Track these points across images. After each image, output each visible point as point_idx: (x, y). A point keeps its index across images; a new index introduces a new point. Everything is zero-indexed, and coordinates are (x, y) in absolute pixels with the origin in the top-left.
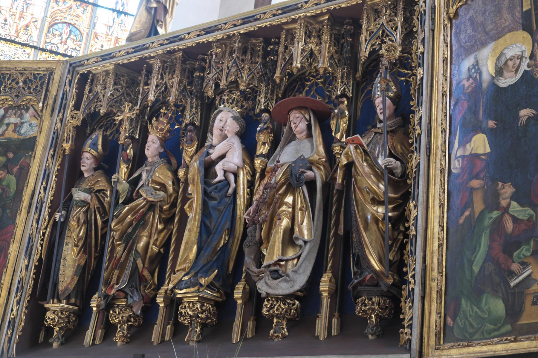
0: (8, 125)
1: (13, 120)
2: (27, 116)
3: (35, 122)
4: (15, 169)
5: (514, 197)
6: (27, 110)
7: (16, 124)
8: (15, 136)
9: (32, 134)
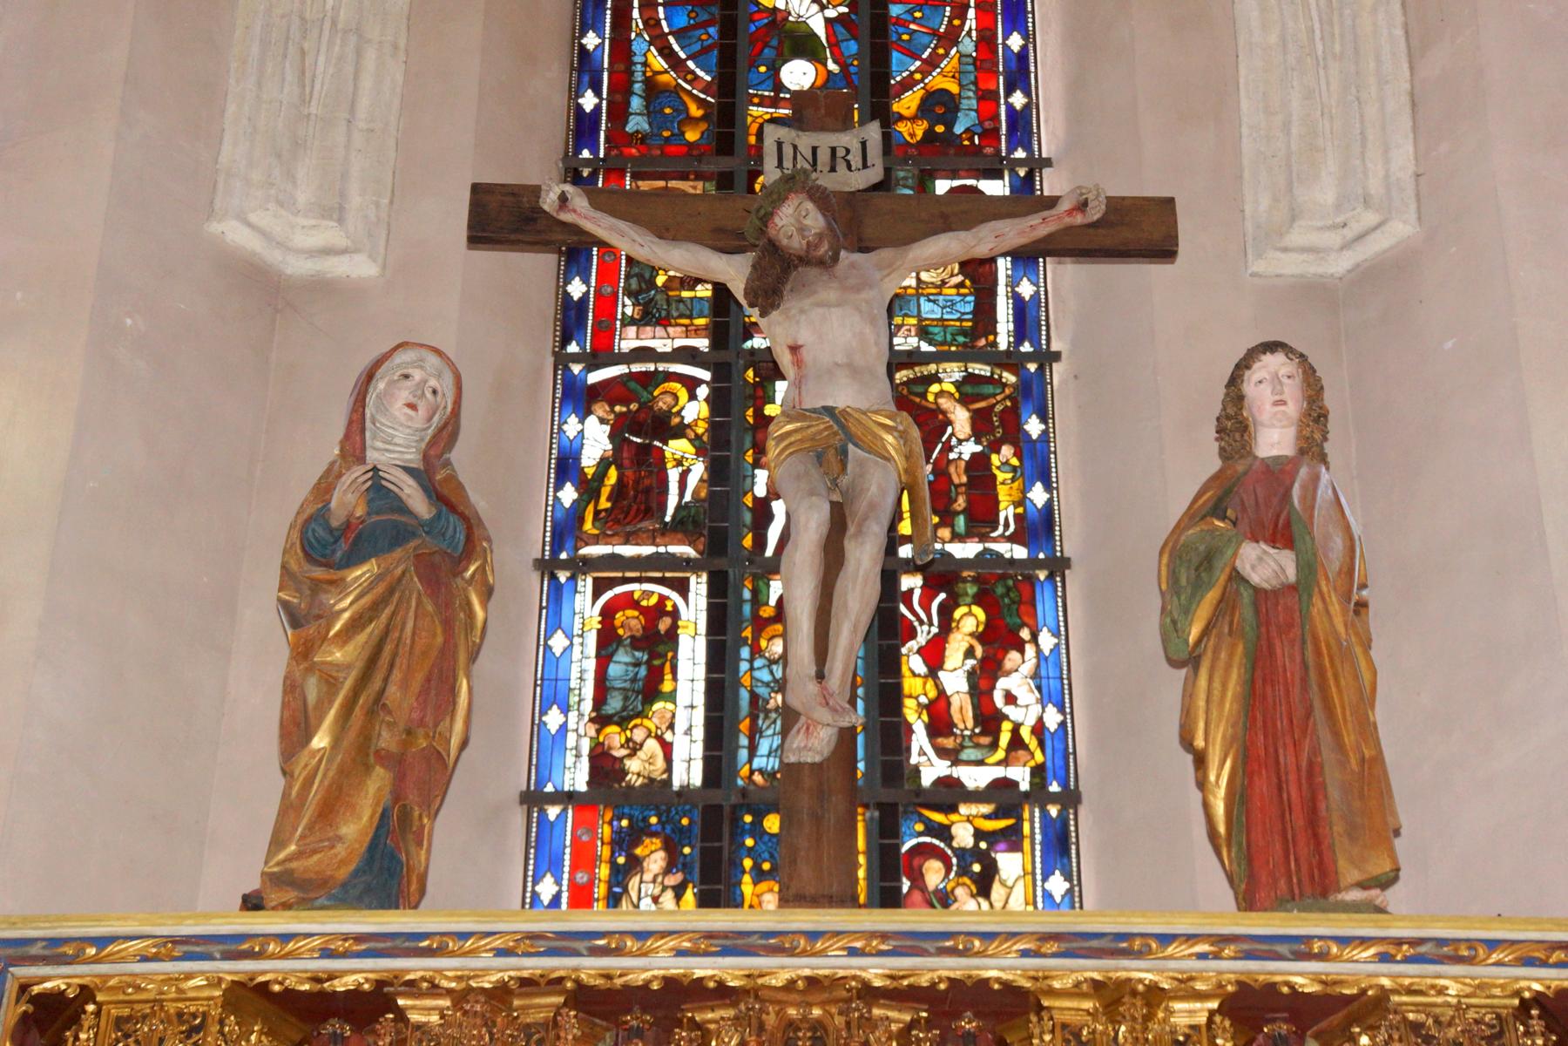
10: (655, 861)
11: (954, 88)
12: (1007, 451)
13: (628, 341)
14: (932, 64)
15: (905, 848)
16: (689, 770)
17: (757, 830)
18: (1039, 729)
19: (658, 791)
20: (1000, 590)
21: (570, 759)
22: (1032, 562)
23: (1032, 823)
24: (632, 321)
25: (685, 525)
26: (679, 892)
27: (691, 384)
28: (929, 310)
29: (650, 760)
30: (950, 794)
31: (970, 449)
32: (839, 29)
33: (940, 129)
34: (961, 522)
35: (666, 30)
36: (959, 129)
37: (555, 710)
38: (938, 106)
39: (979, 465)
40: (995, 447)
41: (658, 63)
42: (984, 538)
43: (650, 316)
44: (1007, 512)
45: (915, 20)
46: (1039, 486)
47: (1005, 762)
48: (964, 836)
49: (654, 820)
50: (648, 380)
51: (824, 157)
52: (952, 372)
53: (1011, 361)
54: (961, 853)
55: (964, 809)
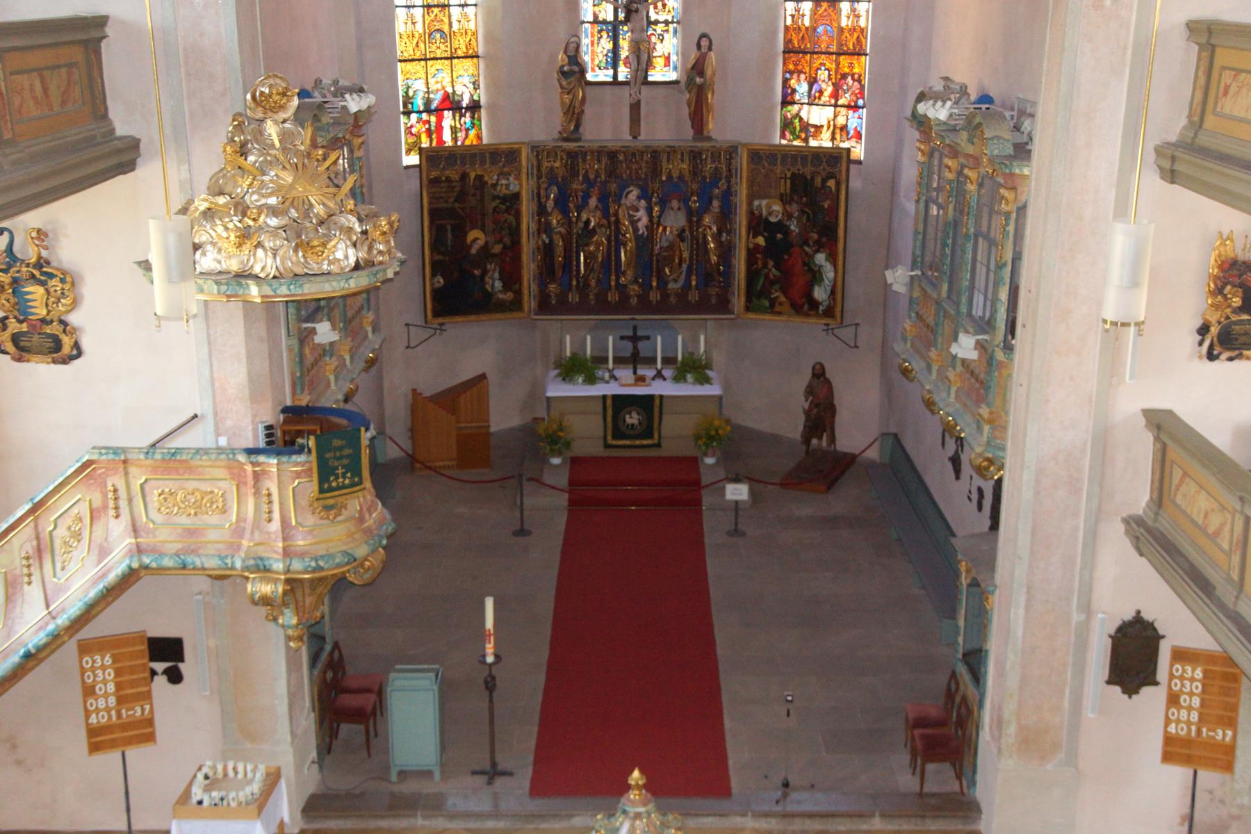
0: (502, 185)
1: (504, 182)
2: (511, 179)
3: (516, 182)
4: (513, 212)
5: (774, 266)
6: (510, 175)
7: (506, 185)
8: (507, 192)
9: (517, 189)
10: (604, 34)
15: (649, 33)
16: (610, 18)
17: (623, 30)
18: (673, 8)
19: (605, 22)
30: (656, 22)
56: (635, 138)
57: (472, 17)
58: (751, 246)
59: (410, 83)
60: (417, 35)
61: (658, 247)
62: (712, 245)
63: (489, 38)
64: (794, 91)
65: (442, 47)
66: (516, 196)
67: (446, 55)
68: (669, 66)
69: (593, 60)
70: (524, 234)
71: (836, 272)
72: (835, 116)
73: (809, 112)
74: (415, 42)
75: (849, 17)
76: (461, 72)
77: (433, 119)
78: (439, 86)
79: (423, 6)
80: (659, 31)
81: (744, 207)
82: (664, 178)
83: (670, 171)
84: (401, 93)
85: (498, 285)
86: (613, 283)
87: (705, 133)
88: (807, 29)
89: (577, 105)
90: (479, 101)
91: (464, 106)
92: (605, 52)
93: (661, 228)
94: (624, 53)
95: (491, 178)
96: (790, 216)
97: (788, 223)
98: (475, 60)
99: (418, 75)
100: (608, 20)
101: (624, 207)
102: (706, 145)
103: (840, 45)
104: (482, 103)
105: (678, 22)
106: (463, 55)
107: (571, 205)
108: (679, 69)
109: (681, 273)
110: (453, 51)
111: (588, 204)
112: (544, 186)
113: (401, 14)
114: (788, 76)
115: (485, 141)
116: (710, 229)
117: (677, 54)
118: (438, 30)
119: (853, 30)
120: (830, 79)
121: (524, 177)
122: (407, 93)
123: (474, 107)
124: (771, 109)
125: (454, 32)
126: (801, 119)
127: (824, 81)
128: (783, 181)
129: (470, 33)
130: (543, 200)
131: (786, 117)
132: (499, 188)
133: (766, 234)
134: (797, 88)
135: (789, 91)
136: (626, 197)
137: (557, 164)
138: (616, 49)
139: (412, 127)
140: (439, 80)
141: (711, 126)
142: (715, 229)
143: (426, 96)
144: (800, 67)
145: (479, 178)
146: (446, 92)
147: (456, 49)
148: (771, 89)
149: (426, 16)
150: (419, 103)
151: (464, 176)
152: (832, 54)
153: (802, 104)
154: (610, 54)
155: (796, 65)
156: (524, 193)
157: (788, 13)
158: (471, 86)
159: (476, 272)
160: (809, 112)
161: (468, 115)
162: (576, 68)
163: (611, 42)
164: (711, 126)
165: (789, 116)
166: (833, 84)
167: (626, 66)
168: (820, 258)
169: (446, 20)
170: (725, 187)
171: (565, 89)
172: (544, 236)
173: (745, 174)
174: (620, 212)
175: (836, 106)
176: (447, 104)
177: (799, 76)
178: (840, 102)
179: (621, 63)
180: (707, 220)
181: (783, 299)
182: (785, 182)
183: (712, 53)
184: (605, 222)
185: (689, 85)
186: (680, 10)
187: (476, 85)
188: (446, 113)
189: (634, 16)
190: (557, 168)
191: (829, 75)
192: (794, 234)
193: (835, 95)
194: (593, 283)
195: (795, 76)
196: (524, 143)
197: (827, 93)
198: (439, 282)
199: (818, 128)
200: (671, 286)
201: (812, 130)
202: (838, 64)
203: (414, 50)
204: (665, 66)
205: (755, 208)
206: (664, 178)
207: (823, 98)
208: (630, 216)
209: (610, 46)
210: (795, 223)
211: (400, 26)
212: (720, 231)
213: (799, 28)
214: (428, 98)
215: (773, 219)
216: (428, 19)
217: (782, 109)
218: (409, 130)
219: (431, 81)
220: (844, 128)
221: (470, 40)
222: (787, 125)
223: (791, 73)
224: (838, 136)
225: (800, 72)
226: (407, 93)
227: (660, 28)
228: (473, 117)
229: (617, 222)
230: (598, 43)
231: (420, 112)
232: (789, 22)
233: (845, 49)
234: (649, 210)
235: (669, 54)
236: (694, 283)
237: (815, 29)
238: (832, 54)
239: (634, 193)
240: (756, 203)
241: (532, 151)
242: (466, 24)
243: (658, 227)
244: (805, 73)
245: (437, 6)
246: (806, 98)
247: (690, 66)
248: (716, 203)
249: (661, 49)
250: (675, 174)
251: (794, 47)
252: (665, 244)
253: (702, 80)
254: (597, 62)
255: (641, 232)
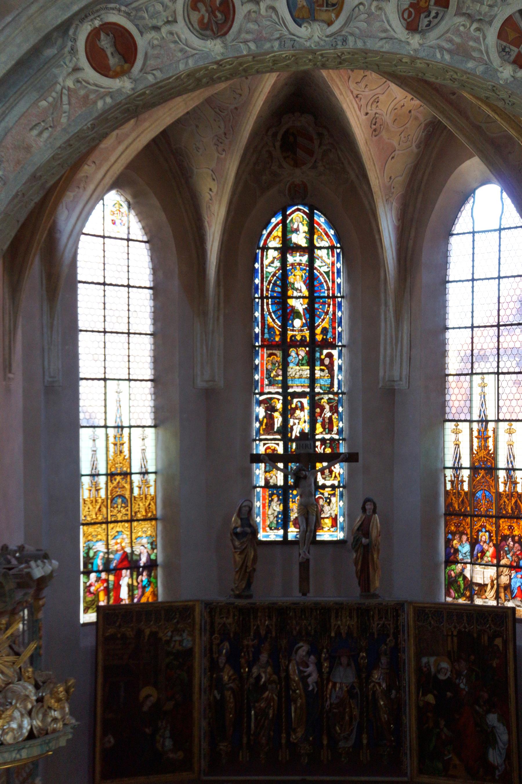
0: (175, 641)
1: (177, 638)
2: (185, 635)
3: (190, 638)
6: (184, 631)
9: (190, 645)
10: (275, 498)
11: (327, 326)
12: (335, 414)
13: (266, 390)
14: (323, 320)
15: (317, 497)
16: (280, 482)
17: (292, 494)
18: (339, 474)
19: (275, 486)
20: (333, 445)
21: (260, 480)
22: (339, 440)
23: (338, 492)
24: (267, 385)
25: (278, 432)
26: (280, 505)
27: (278, 400)
28: (322, 382)
29: (274, 480)
30: (324, 487)
31: (328, 414)
32: (305, 311)
33: (325, 337)
34: (327, 430)
35: (270, 300)
36: (328, 337)
37: (258, 470)
38: (325, 331)
39: (330, 418)
40: (333, 414)
41: (270, 320)
42: (331, 434)
43: (271, 384)
44: (335, 429)
45: (320, 309)
46: (341, 422)
47: (333, 480)
48: (326, 495)
49: (275, 492)
50: (271, 399)
51: (304, 445)
52: (326, 397)
53: (337, 394)
54: (325, 498)
55: (326, 489)
56: (304, 594)
57: (152, 483)
58: (421, 704)
59: (91, 544)
60: (100, 501)
61: (328, 703)
62: (382, 703)
63: (168, 502)
64: (457, 551)
65: (123, 511)
66: (190, 652)
67: (126, 518)
68: (336, 526)
69: (264, 521)
70: (196, 689)
71: (510, 733)
72: (499, 575)
73: (472, 571)
74: (98, 507)
75: (506, 484)
76: (140, 534)
77: (112, 578)
78: (118, 547)
79: (107, 475)
80: (326, 495)
81: (413, 664)
82: (333, 634)
83: (339, 627)
84: (82, 554)
85: (168, 743)
86: (283, 741)
87: (372, 590)
88: (466, 493)
89: (249, 564)
90: (156, 560)
91: (142, 564)
92: (276, 514)
93: (330, 684)
94: (294, 515)
95: (165, 635)
96: (459, 674)
97: (457, 681)
98: (154, 522)
99: (99, 537)
100: (279, 484)
101: (294, 662)
102: (373, 602)
103: (499, 509)
104: (160, 561)
105: (344, 487)
106: (142, 518)
107: (243, 661)
108: (346, 529)
109: (352, 730)
110: (133, 514)
111: (259, 659)
112: (216, 642)
113: (86, 481)
114: (450, 536)
115: (160, 599)
116: (380, 685)
117: (344, 517)
118: (120, 496)
119: (511, 495)
120: (491, 540)
121: (197, 632)
122: (88, 553)
123: (151, 565)
124: (436, 566)
125: (135, 497)
126: (465, 578)
127: (485, 542)
128: (449, 638)
129: (149, 498)
130: (215, 656)
131: (450, 576)
132: (172, 645)
133: (435, 692)
134: (460, 548)
135: (452, 551)
136: (296, 653)
137: (230, 620)
138: (286, 511)
139: (91, 585)
140: (119, 541)
141: (377, 584)
142: (384, 686)
143: (106, 556)
144: (461, 529)
145: (154, 634)
146: (125, 552)
147: (136, 513)
148: (434, 548)
149: (109, 484)
150: (99, 562)
151: (140, 633)
152: (492, 517)
153: (466, 563)
154: (280, 516)
155: (457, 526)
156: (197, 649)
157: (448, 478)
158: (149, 546)
159: (147, 730)
160: (472, 571)
161: (145, 574)
162: (248, 530)
163: (282, 505)
164: (377, 584)
165: (453, 574)
166: (494, 545)
167: (295, 527)
168: (492, 719)
169: (127, 486)
170: (393, 644)
171: (238, 548)
172: (216, 692)
173: (412, 632)
174: (290, 667)
175: (498, 566)
176: (125, 563)
177: (460, 538)
178: (503, 562)
179: (291, 523)
180: (376, 675)
181: (456, 761)
182: (452, 639)
183: (376, 515)
184: (275, 677)
185: (356, 544)
186: (346, 476)
187: (153, 545)
188: (124, 572)
189: (303, 483)
190: (230, 624)
191: (490, 537)
192: (464, 692)
193: (497, 556)
194: (264, 741)
195: (457, 537)
196: (197, 601)
197: (488, 554)
198: (110, 742)
199: (483, 587)
200: (341, 744)
201: (477, 588)
202: (498, 527)
203: (96, 514)
204: (332, 526)
205: (423, 664)
206: (333, 634)
207: (485, 559)
208: (301, 672)
209: (280, 508)
210: (464, 681)
211: (85, 494)
212: (389, 688)
213: (459, 493)
214: (108, 558)
215: (442, 677)
216: (111, 486)
217: (446, 568)
218: (87, 588)
219: (112, 542)
220: (508, 587)
221: (150, 504)
222: (451, 582)
223: (453, 534)
224: (502, 595)
225: (462, 533)
226: (88, 553)
227: (327, 492)
228: (149, 576)
229: (288, 677)
230: (269, 506)
231: (99, 572)
232: (449, 487)
233: (504, 512)
234: (319, 666)
235: (336, 515)
236: (365, 742)
237: (474, 494)
238: (492, 517)
239: (303, 649)
240: (424, 660)
241: (205, 608)
242: (146, 489)
243: (328, 684)
244: (467, 534)
245: (120, 474)
246: (469, 557)
247: (356, 527)
248: (384, 660)
249: (327, 511)
250: (344, 631)
251: (454, 509)
252: (334, 700)
253: (367, 540)
254: (268, 523)
255: (311, 688)
